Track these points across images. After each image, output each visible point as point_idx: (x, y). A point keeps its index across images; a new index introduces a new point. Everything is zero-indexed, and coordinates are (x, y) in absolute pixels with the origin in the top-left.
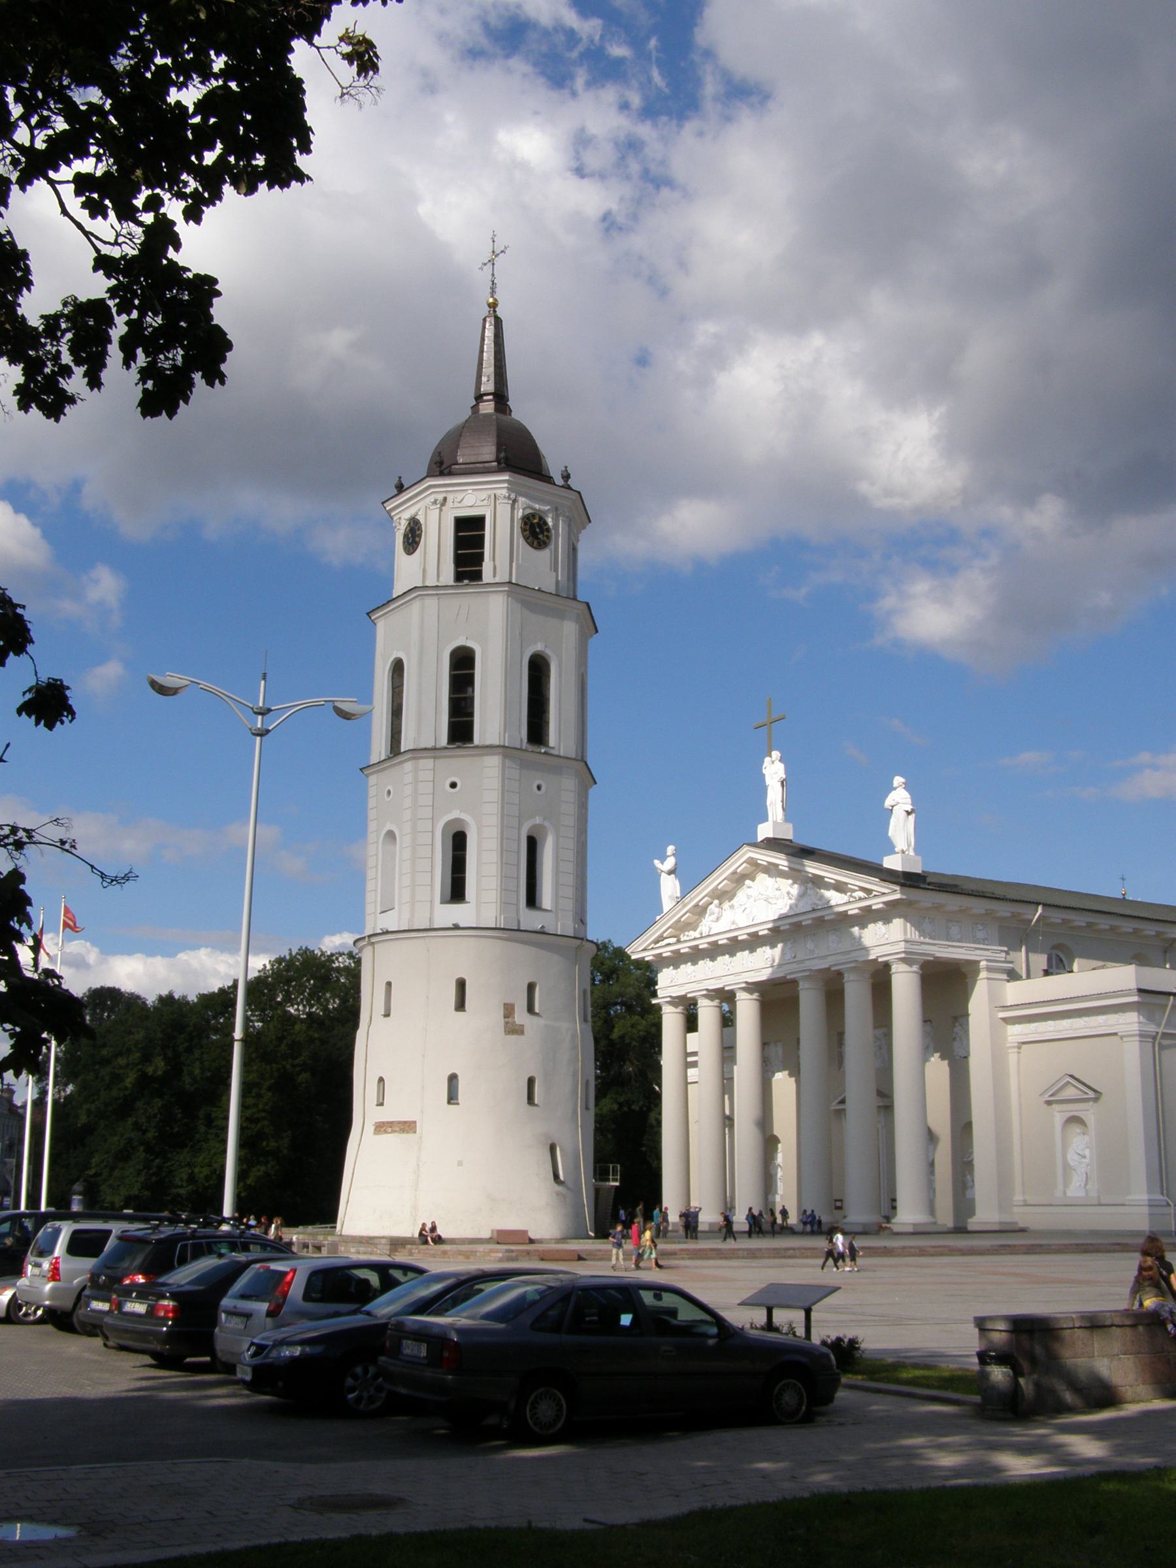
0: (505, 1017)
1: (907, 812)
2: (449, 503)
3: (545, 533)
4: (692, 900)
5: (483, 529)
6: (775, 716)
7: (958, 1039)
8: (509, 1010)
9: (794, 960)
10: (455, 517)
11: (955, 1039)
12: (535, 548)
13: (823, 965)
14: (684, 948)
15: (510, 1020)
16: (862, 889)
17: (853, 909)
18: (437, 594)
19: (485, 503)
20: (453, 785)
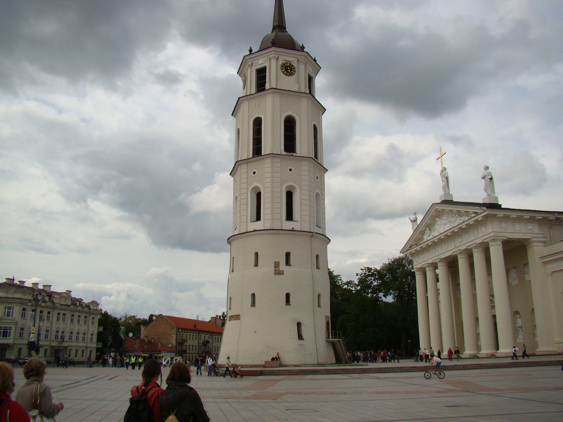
0: (275, 268)
1: (489, 178)
2: (254, 65)
3: (293, 70)
4: (419, 229)
5: (266, 72)
6: (443, 153)
7: (526, 273)
8: (277, 264)
9: (455, 247)
10: (256, 69)
11: (525, 273)
12: (288, 76)
13: (464, 247)
14: (418, 248)
15: (277, 269)
16: (474, 213)
17: (471, 222)
18: (247, 99)
19: (266, 61)
20: (254, 173)
